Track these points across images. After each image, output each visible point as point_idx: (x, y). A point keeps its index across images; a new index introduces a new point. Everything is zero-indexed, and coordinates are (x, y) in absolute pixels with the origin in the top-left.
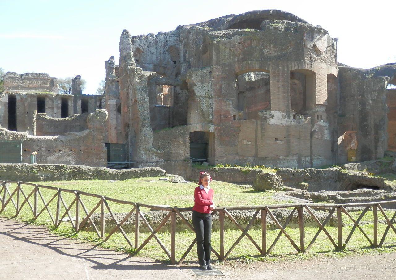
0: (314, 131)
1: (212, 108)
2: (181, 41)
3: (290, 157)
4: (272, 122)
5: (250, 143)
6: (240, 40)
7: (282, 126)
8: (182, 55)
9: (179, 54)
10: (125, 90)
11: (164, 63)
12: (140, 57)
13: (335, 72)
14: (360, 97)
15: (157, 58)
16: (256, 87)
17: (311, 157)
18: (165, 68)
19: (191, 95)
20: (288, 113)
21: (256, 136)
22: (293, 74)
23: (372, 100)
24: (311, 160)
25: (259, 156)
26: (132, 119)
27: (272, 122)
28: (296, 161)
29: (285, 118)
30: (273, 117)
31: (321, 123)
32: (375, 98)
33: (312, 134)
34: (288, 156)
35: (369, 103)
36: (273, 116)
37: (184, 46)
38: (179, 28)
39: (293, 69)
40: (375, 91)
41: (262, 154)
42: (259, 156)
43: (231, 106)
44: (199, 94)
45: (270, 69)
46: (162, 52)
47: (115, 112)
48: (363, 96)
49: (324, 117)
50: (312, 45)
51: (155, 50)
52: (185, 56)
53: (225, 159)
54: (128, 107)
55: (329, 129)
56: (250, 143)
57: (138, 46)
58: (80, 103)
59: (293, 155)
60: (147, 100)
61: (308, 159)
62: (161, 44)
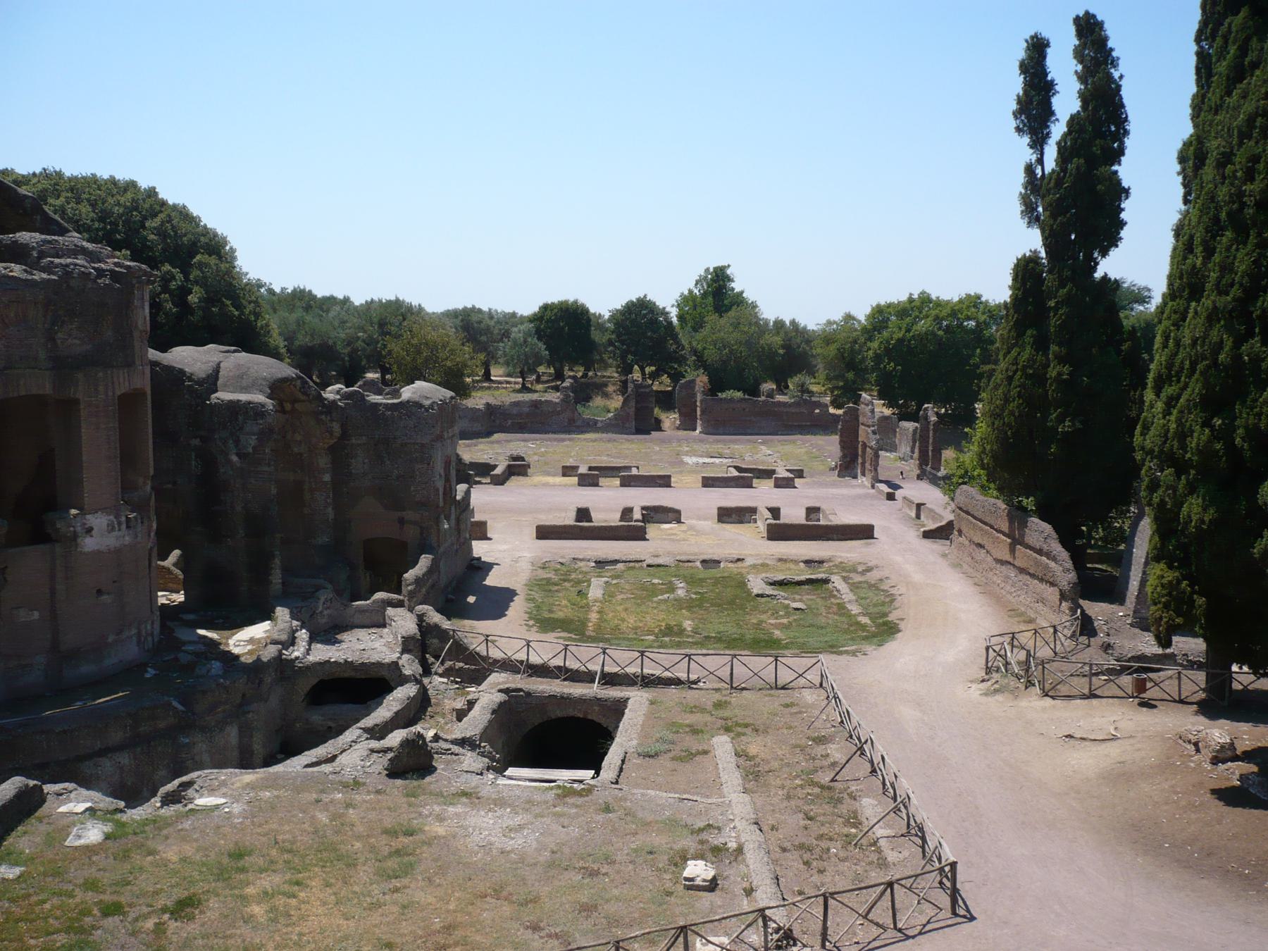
4: (89, 544)
5: (36, 615)
14: (196, 442)
21: (53, 591)
29: (113, 529)
32: (251, 450)
35: (229, 461)
36: (89, 531)
56: (36, 615)
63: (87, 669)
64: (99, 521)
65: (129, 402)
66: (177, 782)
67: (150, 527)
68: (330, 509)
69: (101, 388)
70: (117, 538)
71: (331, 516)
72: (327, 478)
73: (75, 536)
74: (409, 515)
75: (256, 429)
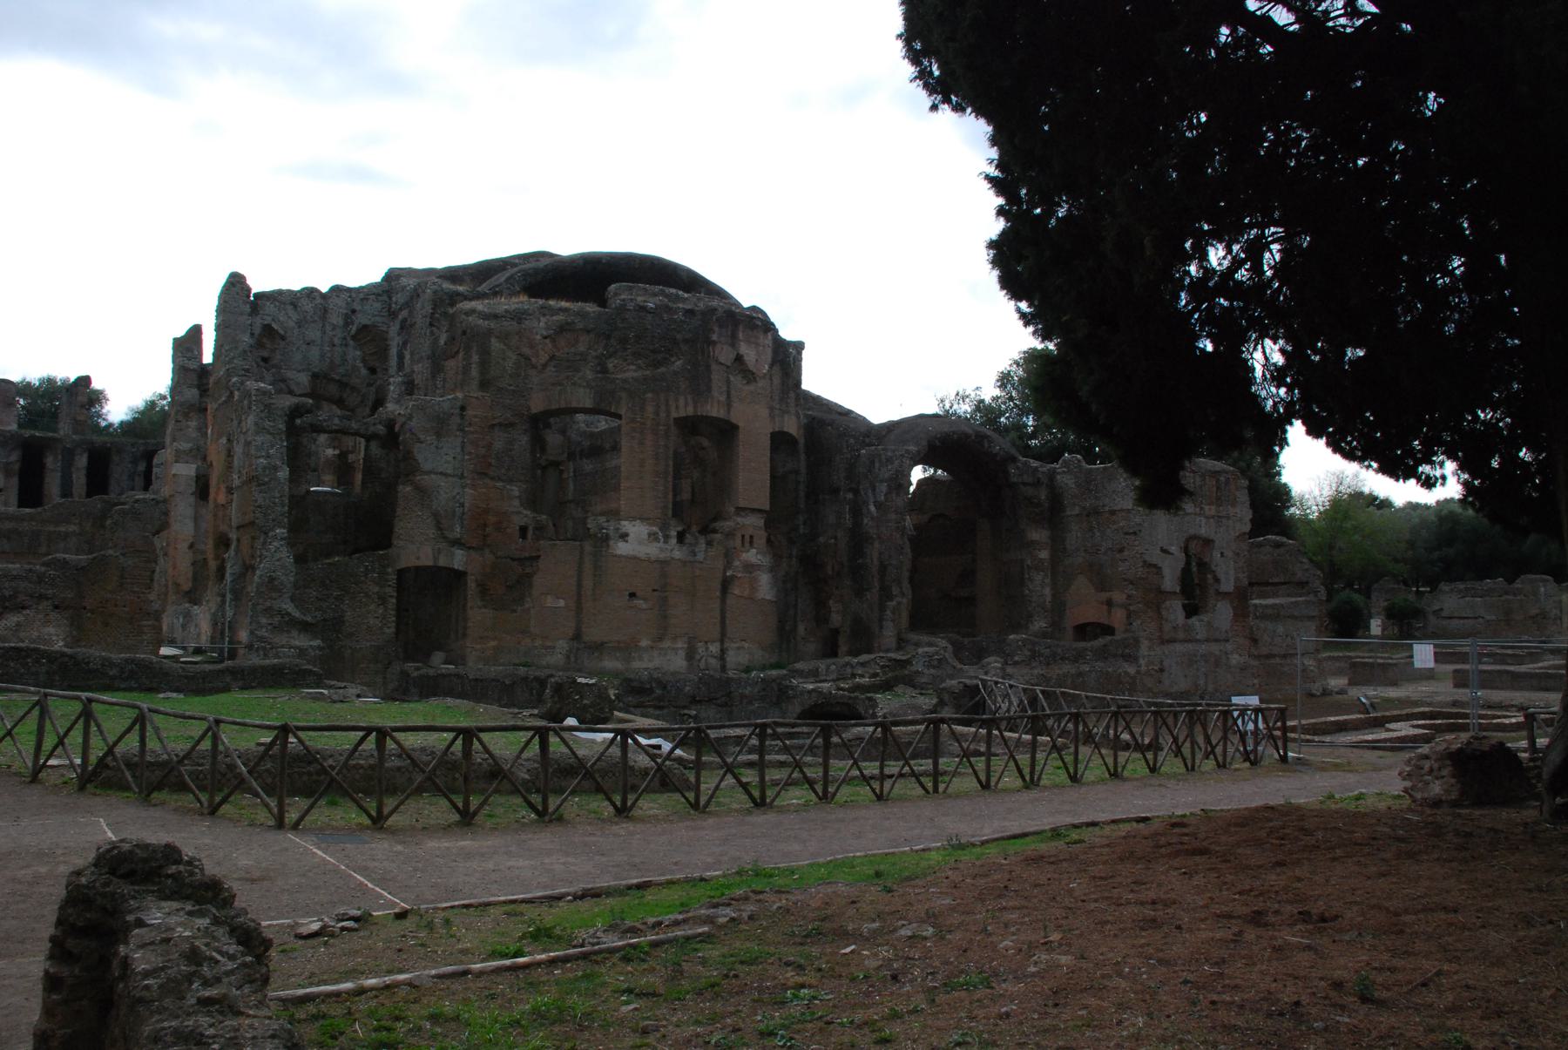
0: (733, 577)
1: (462, 505)
2: (393, 315)
3: (667, 644)
4: (622, 548)
6: (547, 328)
7: (649, 560)
8: (394, 351)
9: (386, 349)
10: (224, 440)
11: (341, 370)
12: (273, 351)
13: (791, 426)
14: (850, 496)
15: (322, 356)
16: (607, 446)
17: (722, 642)
18: (343, 385)
19: (407, 467)
20: (664, 527)
21: (579, 585)
22: (690, 426)
24: (723, 651)
25: (586, 639)
26: (238, 528)
27: (622, 548)
28: (682, 653)
29: (657, 540)
30: (624, 536)
31: (752, 556)
33: (726, 585)
34: (661, 639)
37: (402, 328)
38: (393, 276)
39: (682, 414)
41: (593, 634)
42: (586, 639)
43: (516, 503)
44: (427, 466)
45: (622, 412)
46: (336, 341)
47: (192, 499)
48: (856, 492)
49: (761, 540)
50: (732, 356)
51: (319, 334)
52: (401, 357)
53: (493, 643)
54: (230, 491)
55: (772, 570)
56: (562, 603)
57: (268, 320)
58: (82, 461)
59: (675, 639)
60: (283, 474)
61: (714, 648)
62: (335, 319)
64: (637, 530)
69: (650, 409)
70: (662, 550)
71: (1049, 599)
72: (1044, 554)
73: (607, 538)
74: (1119, 597)
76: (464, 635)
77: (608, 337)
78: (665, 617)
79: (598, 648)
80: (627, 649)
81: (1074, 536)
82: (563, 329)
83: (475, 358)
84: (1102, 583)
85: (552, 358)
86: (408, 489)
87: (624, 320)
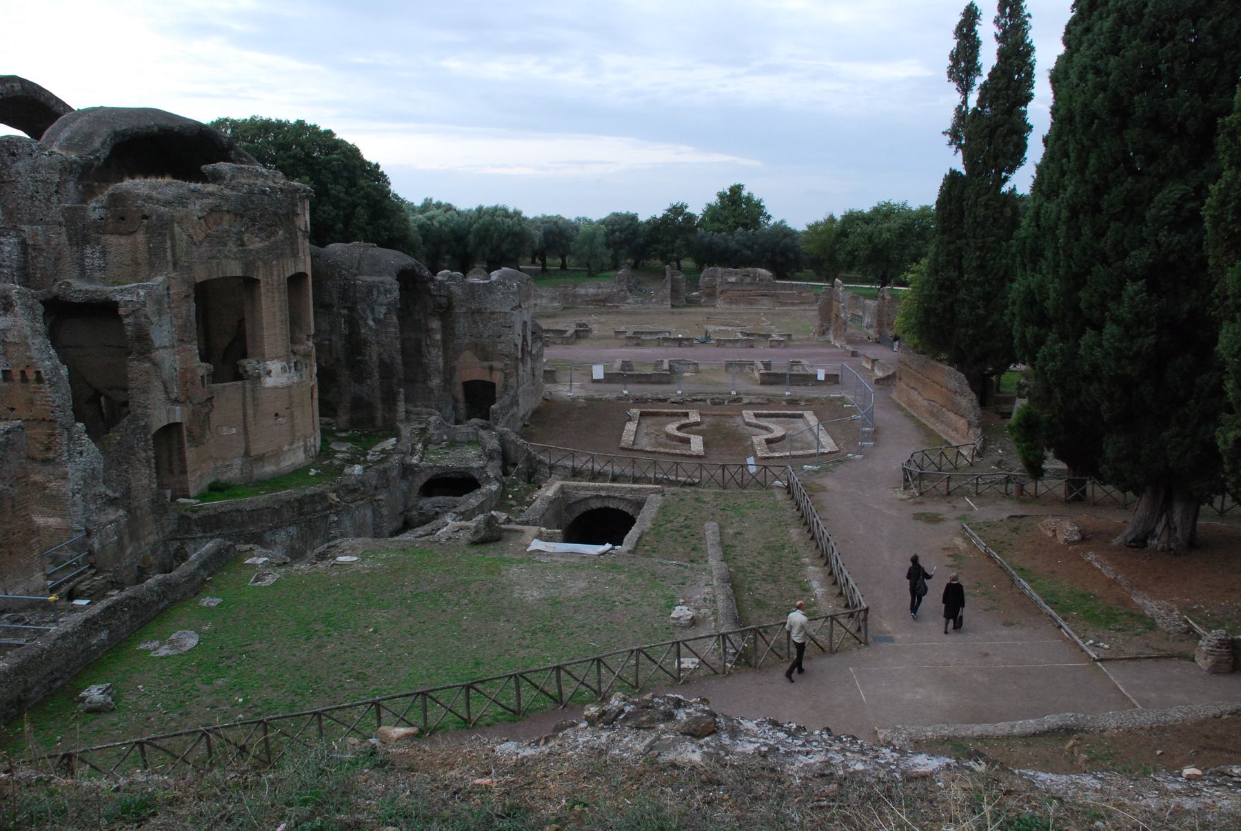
3: (296, 445)
4: (269, 382)
5: (234, 431)
6: (202, 210)
14: (345, 312)
20: (288, 363)
21: (245, 415)
23: (374, 320)
30: (269, 373)
34: (292, 444)
35: (367, 324)
40: (381, 305)
41: (256, 449)
42: (252, 454)
56: (234, 431)
63: (269, 469)
64: (275, 366)
65: (296, 281)
66: (326, 545)
67: (311, 372)
68: (440, 360)
69: (275, 273)
72: (438, 337)
73: (259, 377)
74: (497, 364)
75: (385, 302)
76: (184, 472)
77: (242, 216)
78: (293, 426)
79: (261, 458)
80: (277, 455)
81: (462, 326)
82: (213, 210)
83: (169, 243)
84: (484, 353)
85: (207, 236)
86: (148, 365)
87: (252, 202)
